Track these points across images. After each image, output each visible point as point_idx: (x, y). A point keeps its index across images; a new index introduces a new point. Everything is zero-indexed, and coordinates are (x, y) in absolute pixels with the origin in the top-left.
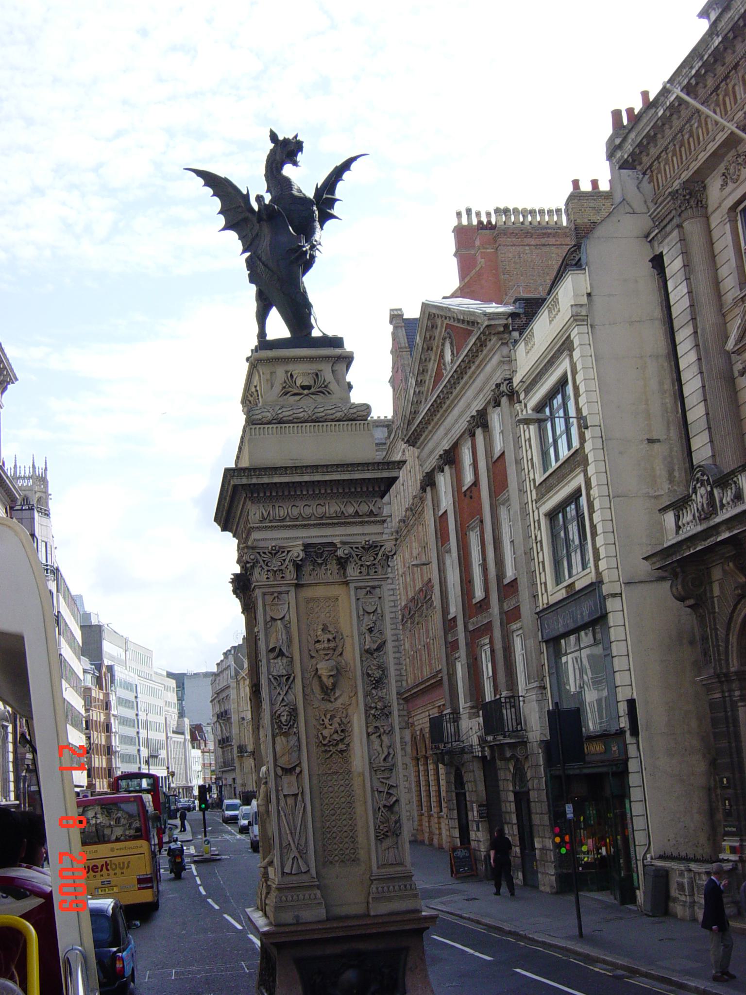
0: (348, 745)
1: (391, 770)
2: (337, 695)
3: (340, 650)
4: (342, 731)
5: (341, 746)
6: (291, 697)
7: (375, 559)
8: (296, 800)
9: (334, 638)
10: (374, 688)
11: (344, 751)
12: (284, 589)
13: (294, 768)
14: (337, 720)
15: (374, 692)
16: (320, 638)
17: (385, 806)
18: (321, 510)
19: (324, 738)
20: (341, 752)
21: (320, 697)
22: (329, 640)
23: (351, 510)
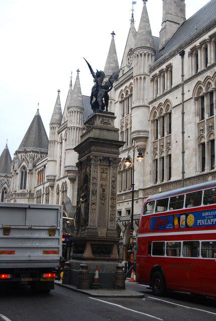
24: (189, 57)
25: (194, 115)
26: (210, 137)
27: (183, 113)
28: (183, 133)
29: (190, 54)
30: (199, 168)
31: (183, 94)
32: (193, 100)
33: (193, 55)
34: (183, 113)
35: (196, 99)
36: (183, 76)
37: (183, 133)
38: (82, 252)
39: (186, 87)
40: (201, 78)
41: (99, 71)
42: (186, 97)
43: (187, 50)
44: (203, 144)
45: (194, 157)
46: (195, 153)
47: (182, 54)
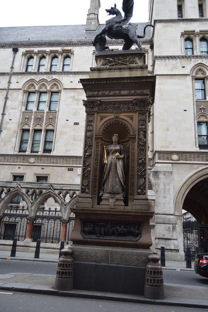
24: (22, 56)
25: (21, 104)
26: (35, 126)
27: (6, 98)
28: (3, 114)
29: (24, 54)
30: (17, 149)
31: (9, 82)
32: (21, 92)
33: (26, 57)
34: (6, 98)
35: (25, 92)
36: (12, 68)
37: (3, 114)
38: (138, 235)
39: (14, 79)
40: (37, 78)
41: (109, 8)
42: (12, 86)
43: (22, 50)
44: (25, 131)
45: (14, 140)
46: (15, 135)
47: (15, 51)
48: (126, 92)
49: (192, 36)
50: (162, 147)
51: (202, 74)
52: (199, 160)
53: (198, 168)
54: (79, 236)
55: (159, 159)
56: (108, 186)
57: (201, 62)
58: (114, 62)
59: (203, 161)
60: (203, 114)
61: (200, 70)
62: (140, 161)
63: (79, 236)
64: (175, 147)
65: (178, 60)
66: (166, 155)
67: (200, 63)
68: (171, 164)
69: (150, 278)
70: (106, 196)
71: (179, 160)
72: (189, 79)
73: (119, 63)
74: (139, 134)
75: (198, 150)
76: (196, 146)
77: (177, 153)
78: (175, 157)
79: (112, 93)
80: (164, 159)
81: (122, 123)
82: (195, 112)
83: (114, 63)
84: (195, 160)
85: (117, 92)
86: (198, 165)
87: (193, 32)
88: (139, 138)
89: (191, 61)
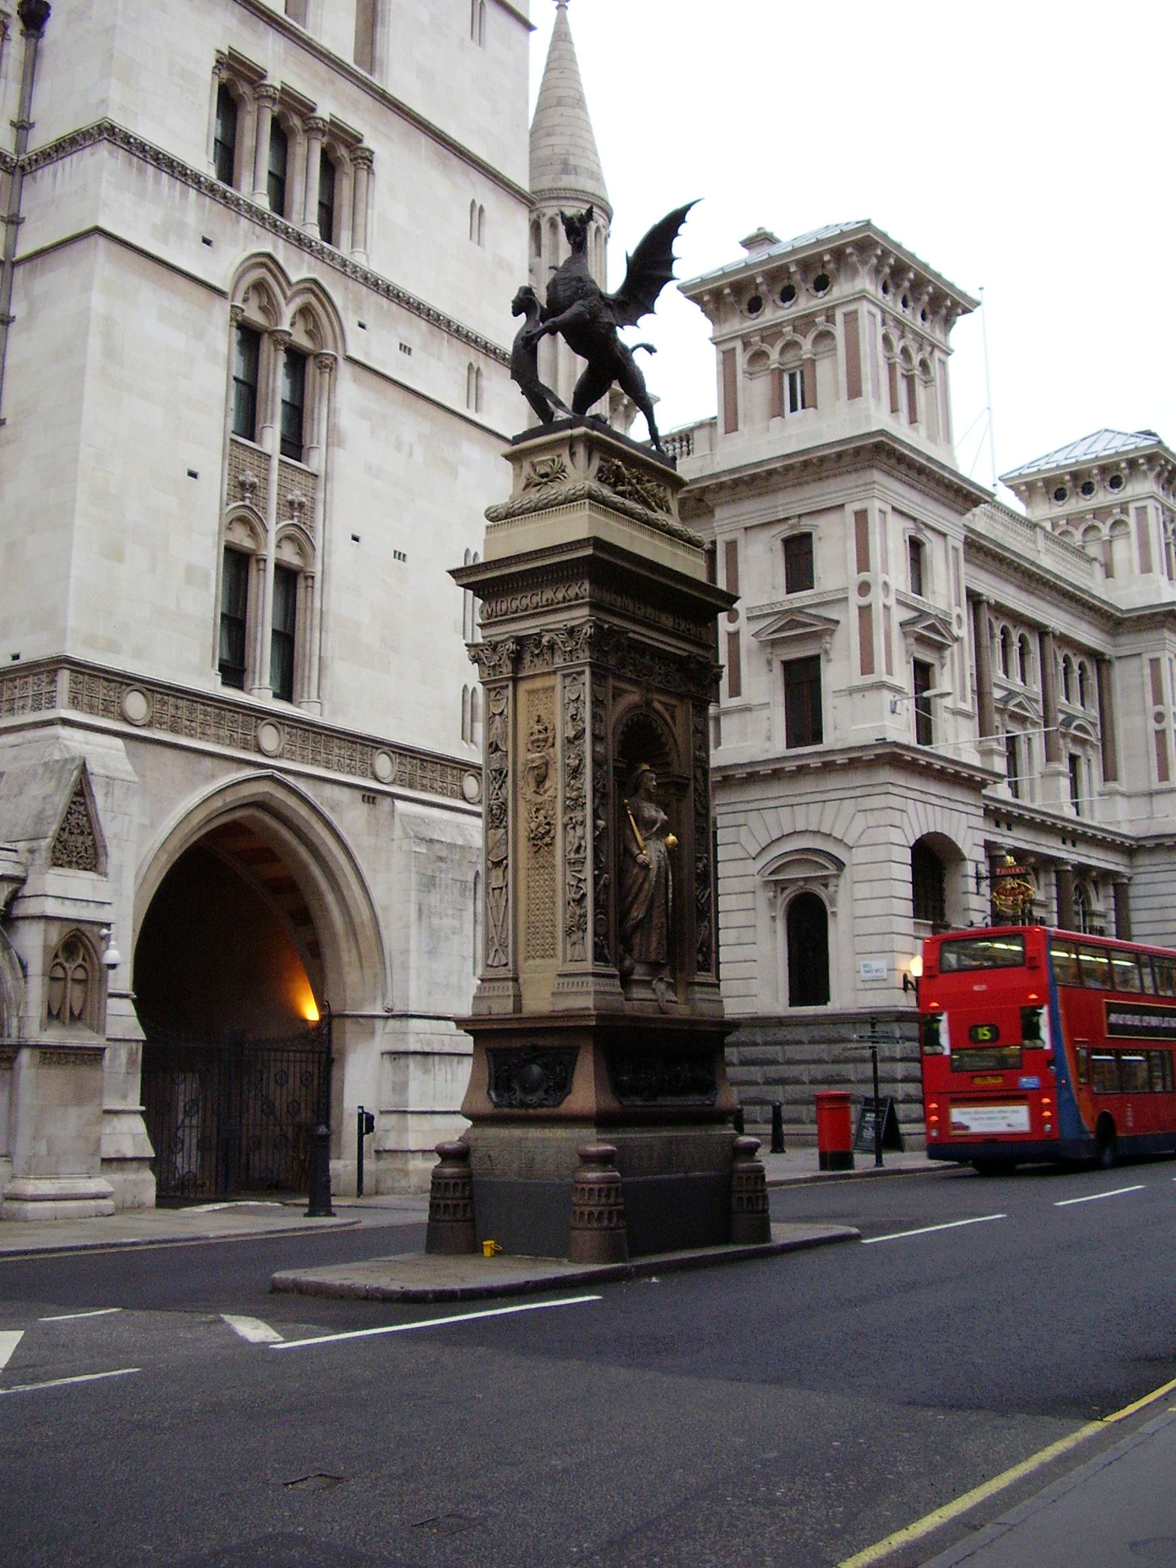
0: (554, 838)
1: (583, 863)
2: (546, 787)
3: (551, 740)
4: (548, 824)
5: (547, 840)
6: (504, 791)
7: (577, 644)
8: (501, 893)
9: (546, 729)
10: (573, 778)
11: (551, 844)
12: (504, 684)
13: (502, 860)
14: (542, 812)
15: (572, 782)
16: (533, 730)
17: (574, 900)
18: (536, 599)
19: (532, 831)
20: (546, 845)
21: (533, 790)
22: (540, 732)
23: (560, 596)
38: (707, 1086)
48: (667, 621)
49: (244, 89)
50: (90, 641)
51: (262, 309)
52: (218, 740)
53: (213, 776)
54: (611, 1103)
55: (75, 703)
56: (649, 942)
57: (268, 249)
58: (630, 483)
59: (232, 743)
60: (298, 533)
61: (260, 287)
62: (700, 865)
63: (611, 1103)
64: (138, 654)
65: (192, 193)
66: (101, 690)
67: (269, 256)
68: (119, 742)
69: (745, 1196)
70: (639, 973)
71: (149, 725)
72: (220, 313)
73: (637, 492)
74: (695, 777)
75: (211, 684)
76: (213, 666)
77: (151, 688)
78: (136, 705)
79: (641, 613)
80: (92, 710)
81: (657, 728)
82: (225, 497)
83: (630, 488)
84: (204, 736)
85: (650, 612)
86: (216, 761)
87: (255, 76)
88: (696, 789)
89: (238, 222)
